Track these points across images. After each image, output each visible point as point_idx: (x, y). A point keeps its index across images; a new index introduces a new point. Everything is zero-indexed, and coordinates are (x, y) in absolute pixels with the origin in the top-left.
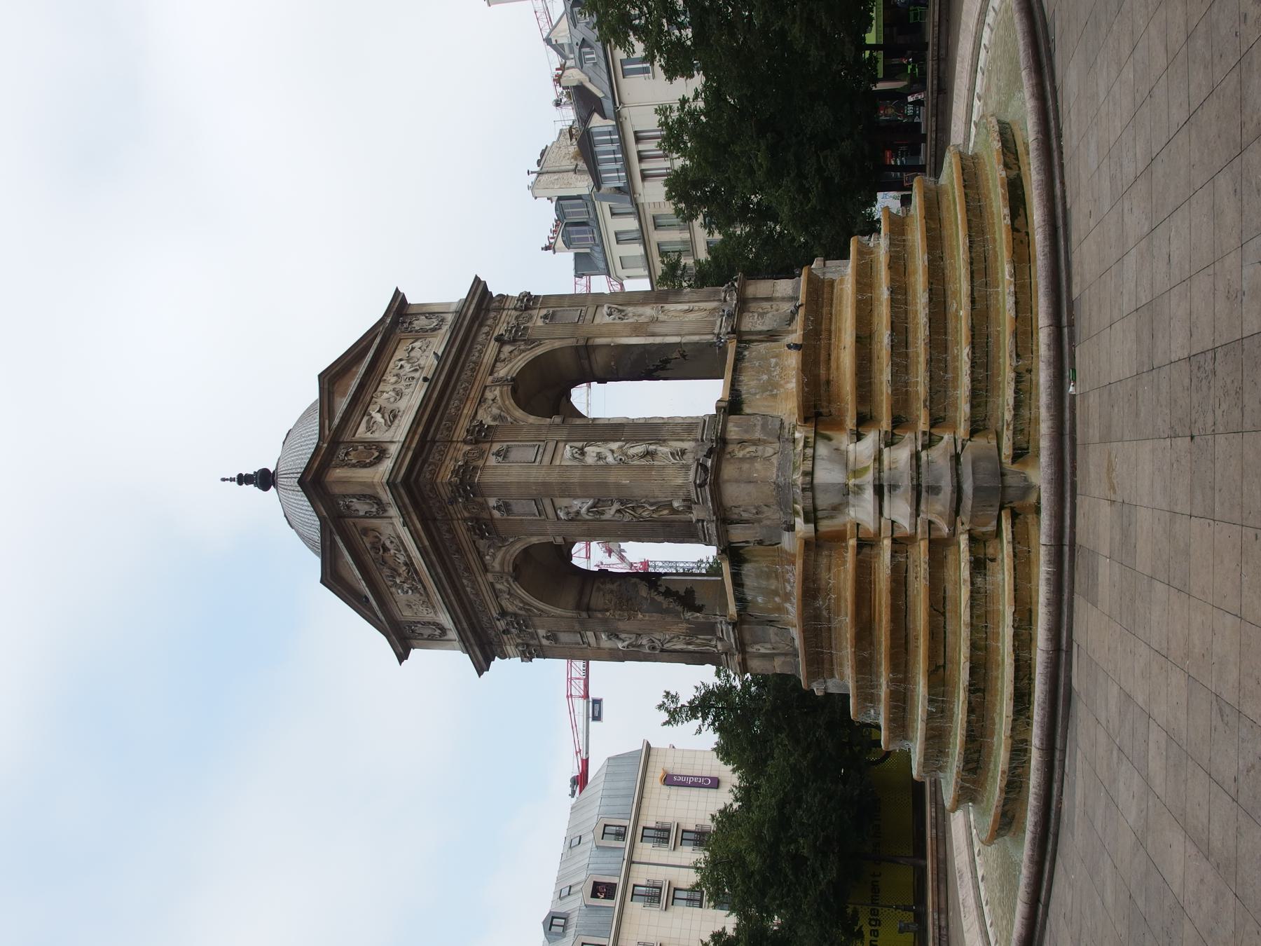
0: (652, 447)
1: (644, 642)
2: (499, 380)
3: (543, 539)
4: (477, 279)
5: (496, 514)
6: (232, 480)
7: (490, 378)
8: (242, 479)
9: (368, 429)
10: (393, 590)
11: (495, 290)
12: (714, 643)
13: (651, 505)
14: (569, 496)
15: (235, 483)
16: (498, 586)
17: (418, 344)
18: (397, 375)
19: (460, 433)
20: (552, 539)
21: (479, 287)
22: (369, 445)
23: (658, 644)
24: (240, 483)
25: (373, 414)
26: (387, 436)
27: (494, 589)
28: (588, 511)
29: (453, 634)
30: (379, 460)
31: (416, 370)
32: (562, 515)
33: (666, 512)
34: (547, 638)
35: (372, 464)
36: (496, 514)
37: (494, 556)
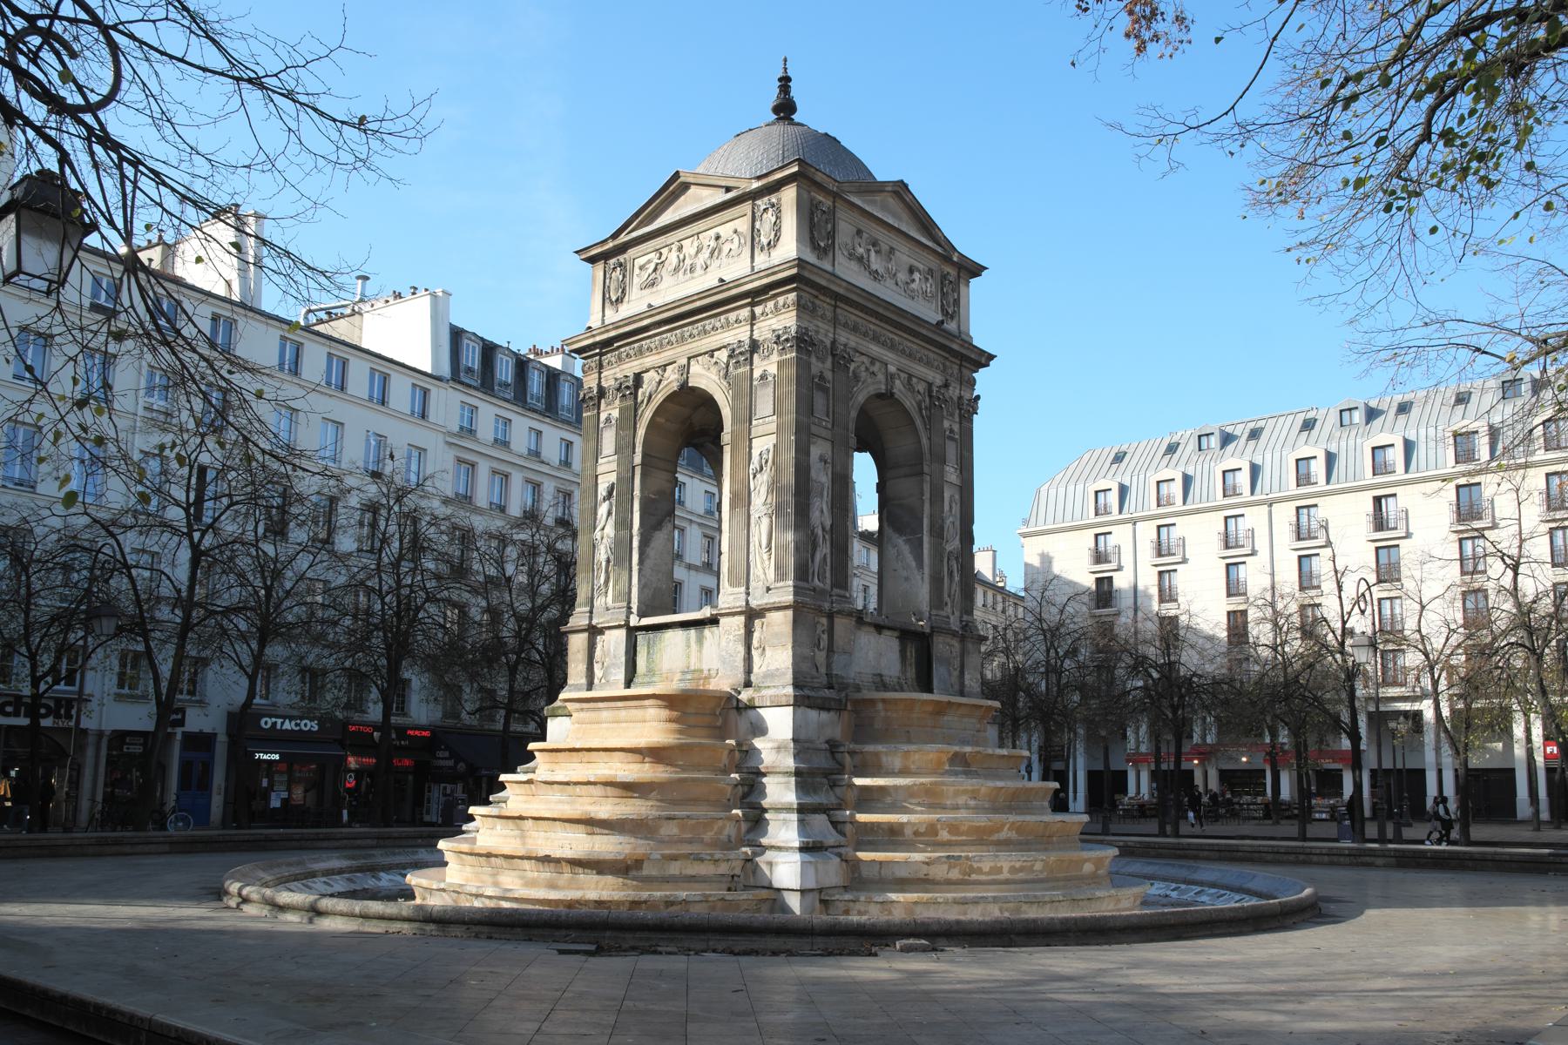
4: (991, 357)
8: (785, 81)
11: (981, 376)
15: (781, 74)
16: (669, 368)
19: (844, 337)
21: (984, 359)
22: (832, 235)
26: (840, 258)
29: (612, 316)
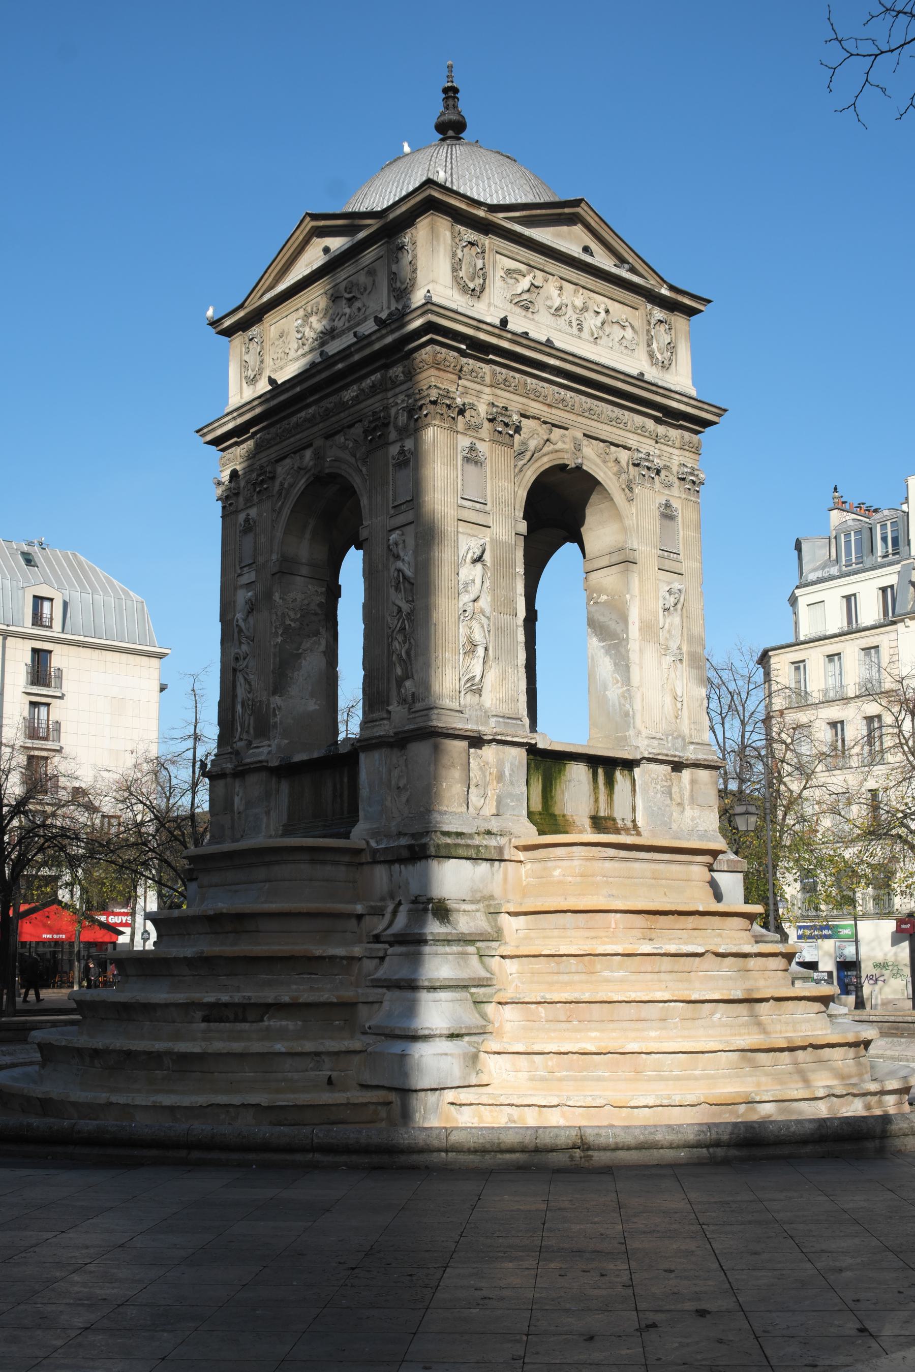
0: (480, 651)
1: (244, 648)
2: (578, 448)
3: (365, 512)
5: (394, 450)
6: (450, 78)
7: (580, 435)
9: (509, 272)
10: (301, 312)
12: (245, 736)
13: (408, 653)
14: (417, 546)
16: (308, 454)
17: (629, 334)
18: (585, 309)
20: (365, 523)
23: (242, 664)
24: (446, 90)
25: (529, 278)
27: (304, 448)
28: (399, 571)
30: (465, 289)
31: (592, 335)
32: (394, 536)
33: (399, 671)
34: (247, 520)
35: (456, 279)
36: (394, 450)
37: (343, 447)
